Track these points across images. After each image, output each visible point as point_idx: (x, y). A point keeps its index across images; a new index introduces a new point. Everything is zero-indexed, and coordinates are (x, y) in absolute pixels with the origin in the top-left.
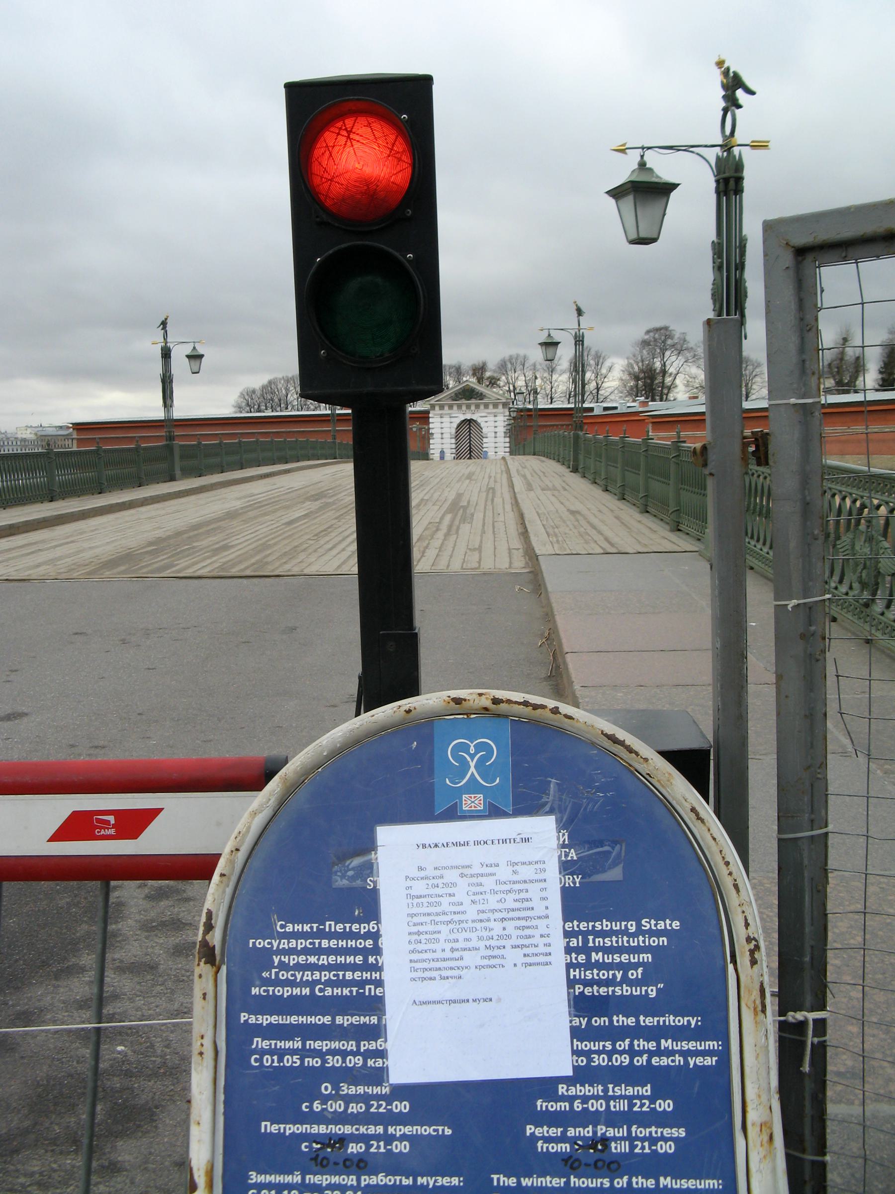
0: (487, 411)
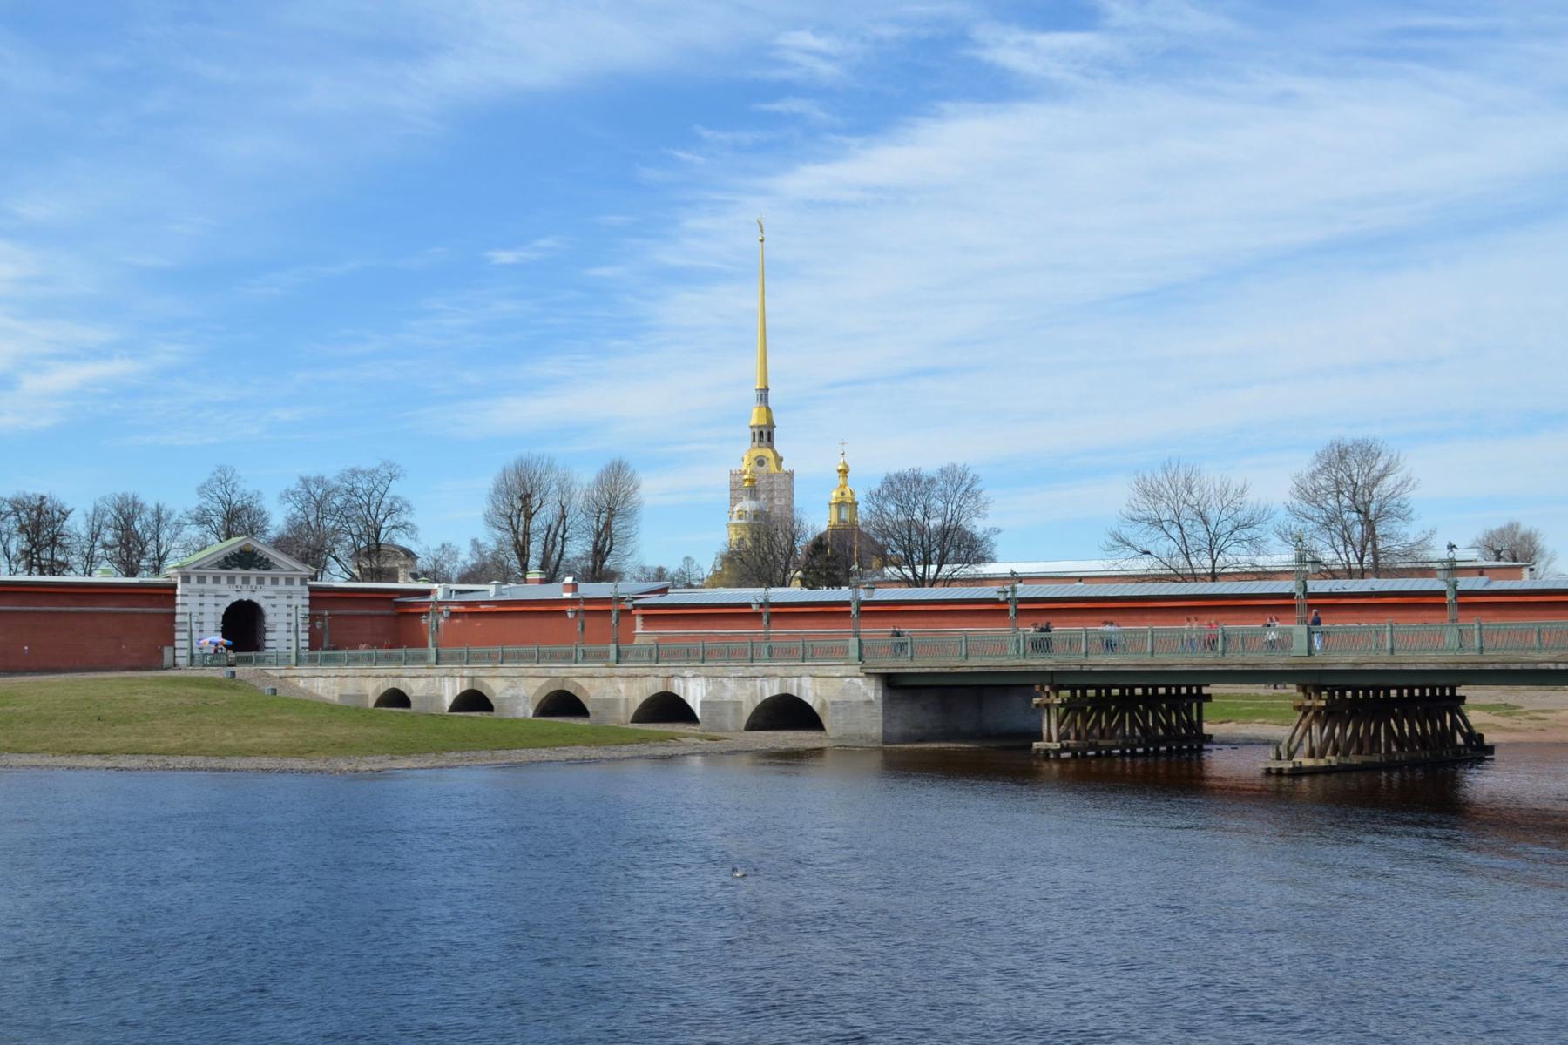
0: (275, 588)
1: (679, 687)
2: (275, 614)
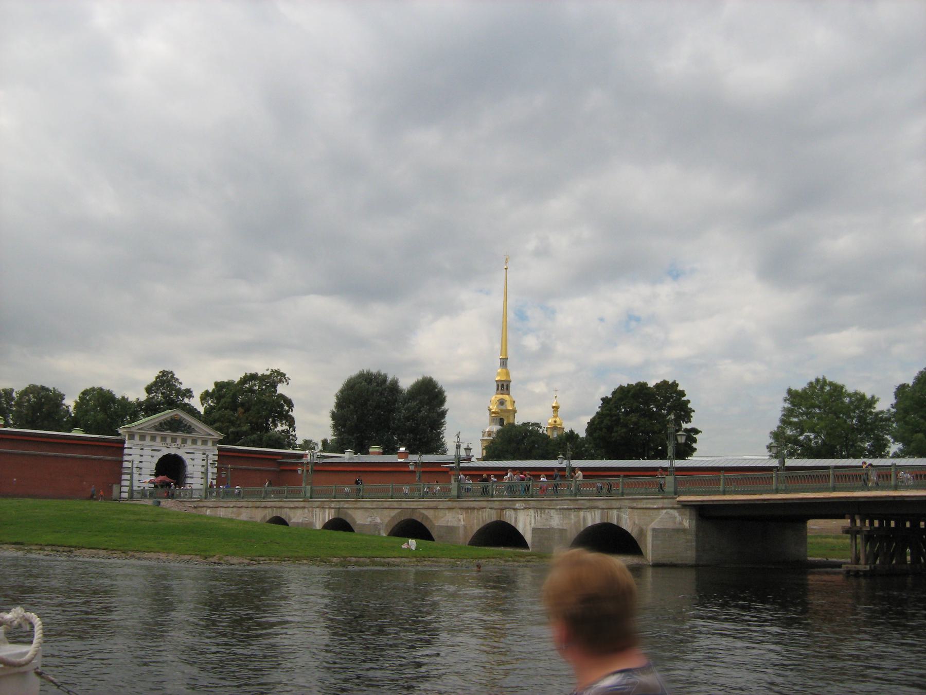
0: (194, 446)
1: (510, 516)
2: (193, 465)
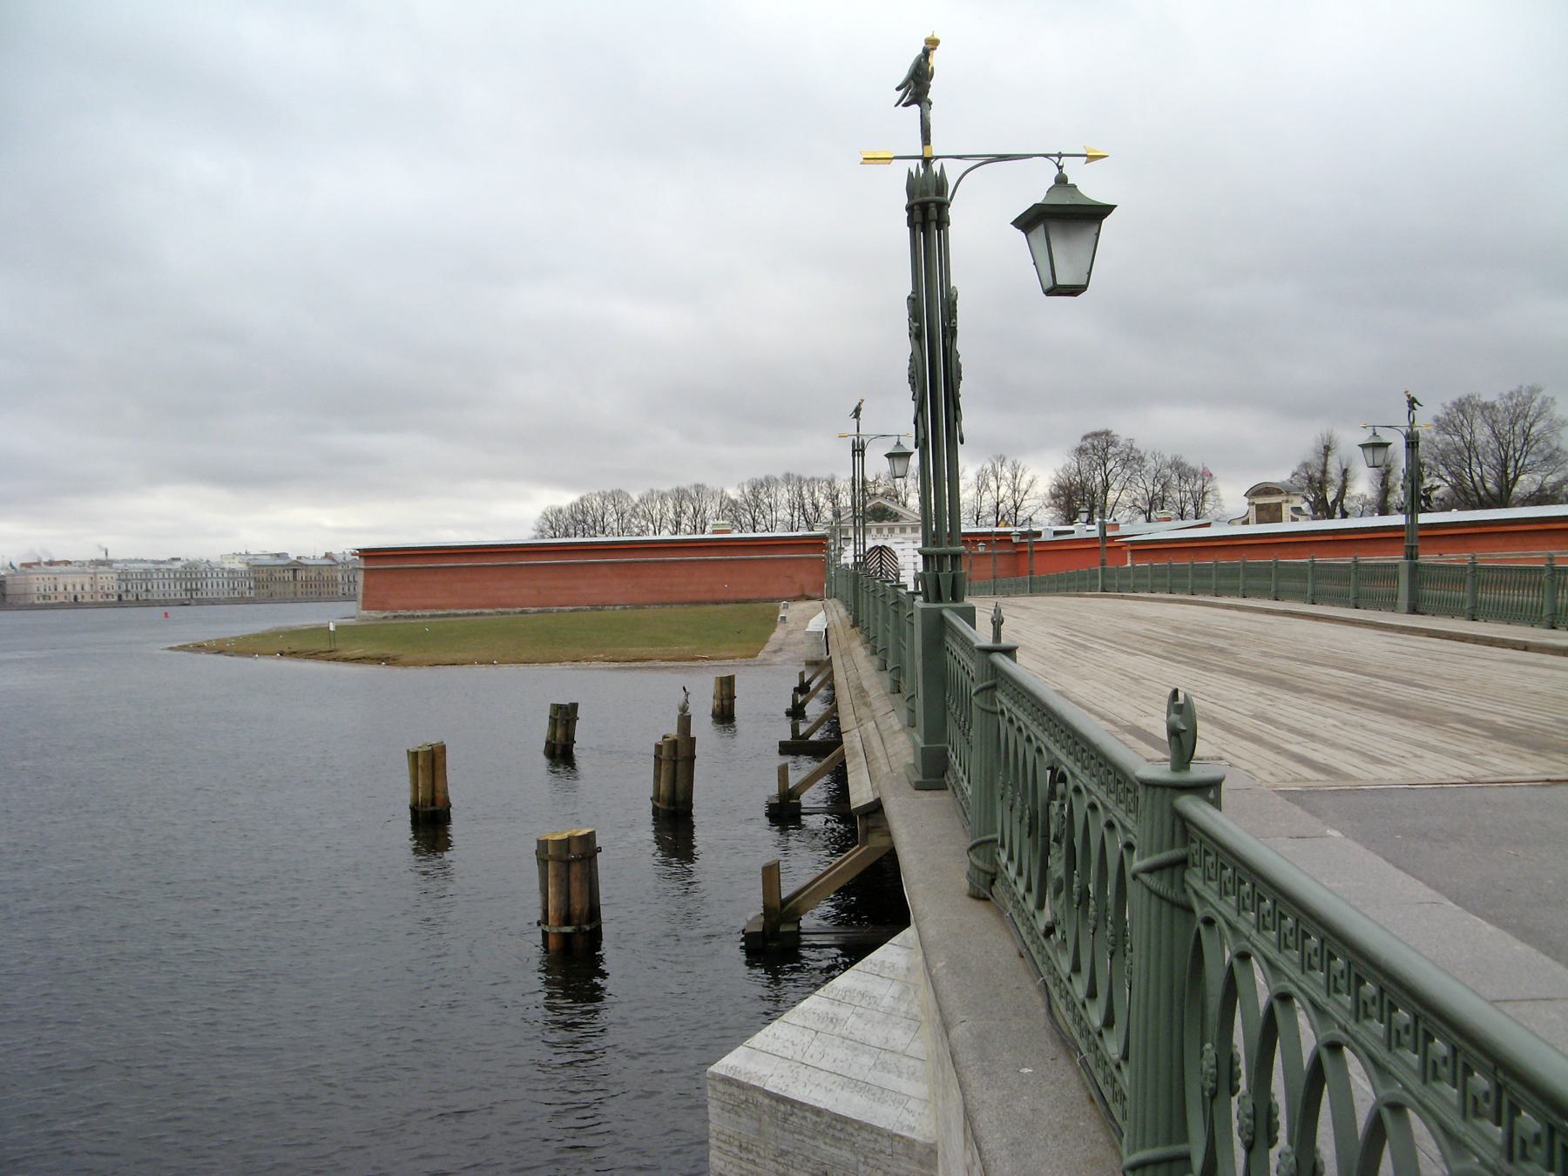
0: (903, 535)
